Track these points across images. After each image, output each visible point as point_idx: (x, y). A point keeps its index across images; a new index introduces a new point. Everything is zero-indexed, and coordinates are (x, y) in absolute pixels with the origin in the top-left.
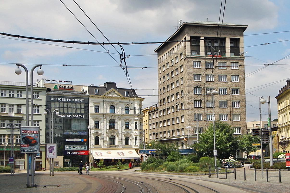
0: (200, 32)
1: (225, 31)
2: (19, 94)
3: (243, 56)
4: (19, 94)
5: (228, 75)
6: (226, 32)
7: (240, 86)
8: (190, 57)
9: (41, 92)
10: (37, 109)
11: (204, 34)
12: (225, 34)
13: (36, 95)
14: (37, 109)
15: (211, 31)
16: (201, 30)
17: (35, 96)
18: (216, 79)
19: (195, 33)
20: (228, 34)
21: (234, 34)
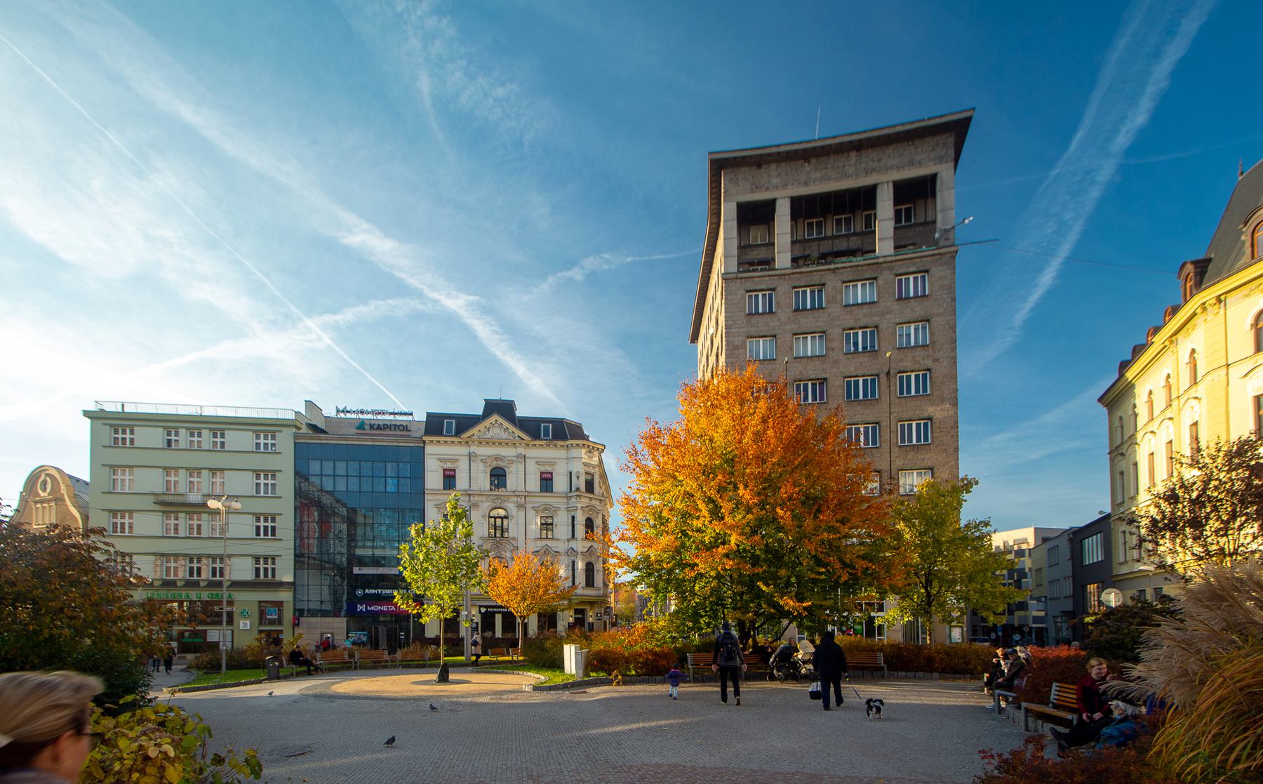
0: (775, 181)
1: (876, 158)
2: (219, 440)
3: (947, 243)
4: (219, 440)
5: (883, 325)
6: (879, 161)
7: (936, 360)
8: (734, 275)
9: (280, 431)
10: (270, 482)
11: (789, 187)
12: (874, 170)
13: (266, 441)
14: (270, 482)
15: (817, 169)
16: (779, 175)
17: (266, 445)
18: (835, 344)
19: (756, 187)
20: (887, 170)
21: (913, 165)
